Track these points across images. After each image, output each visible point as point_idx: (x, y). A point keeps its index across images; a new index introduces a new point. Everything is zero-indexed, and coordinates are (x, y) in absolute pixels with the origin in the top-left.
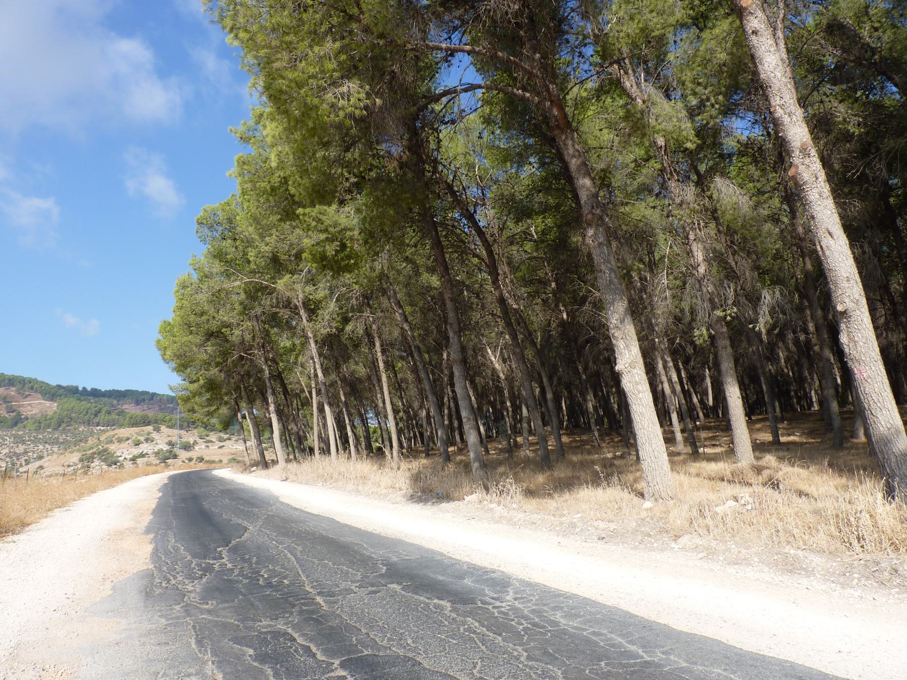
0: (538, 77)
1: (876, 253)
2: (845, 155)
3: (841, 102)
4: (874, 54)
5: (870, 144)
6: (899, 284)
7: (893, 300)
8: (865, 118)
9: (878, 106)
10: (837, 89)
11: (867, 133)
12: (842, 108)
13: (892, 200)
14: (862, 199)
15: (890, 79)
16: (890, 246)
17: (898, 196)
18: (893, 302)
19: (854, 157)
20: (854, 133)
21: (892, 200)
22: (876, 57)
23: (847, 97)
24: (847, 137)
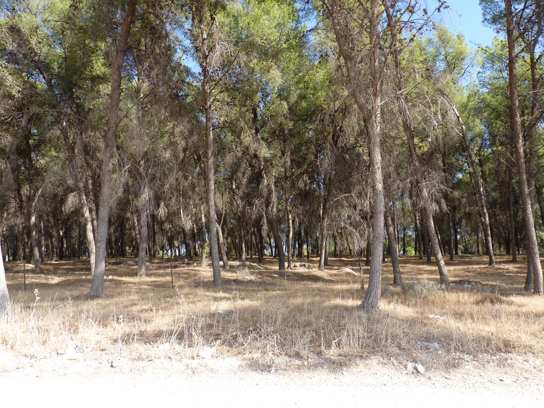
0: (171, 67)
1: (16, 170)
2: (7, 107)
3: (10, 74)
4: (35, 56)
5: (24, 105)
6: (27, 190)
7: (22, 199)
8: (24, 89)
9: (33, 86)
10: (10, 66)
11: (23, 99)
12: (10, 78)
13: (31, 141)
14: (14, 135)
15: (42, 73)
16: (25, 167)
17: (35, 140)
18: (21, 201)
19: (12, 109)
20: (14, 95)
21: (31, 141)
22: (36, 58)
23: (16, 73)
24: (11, 97)
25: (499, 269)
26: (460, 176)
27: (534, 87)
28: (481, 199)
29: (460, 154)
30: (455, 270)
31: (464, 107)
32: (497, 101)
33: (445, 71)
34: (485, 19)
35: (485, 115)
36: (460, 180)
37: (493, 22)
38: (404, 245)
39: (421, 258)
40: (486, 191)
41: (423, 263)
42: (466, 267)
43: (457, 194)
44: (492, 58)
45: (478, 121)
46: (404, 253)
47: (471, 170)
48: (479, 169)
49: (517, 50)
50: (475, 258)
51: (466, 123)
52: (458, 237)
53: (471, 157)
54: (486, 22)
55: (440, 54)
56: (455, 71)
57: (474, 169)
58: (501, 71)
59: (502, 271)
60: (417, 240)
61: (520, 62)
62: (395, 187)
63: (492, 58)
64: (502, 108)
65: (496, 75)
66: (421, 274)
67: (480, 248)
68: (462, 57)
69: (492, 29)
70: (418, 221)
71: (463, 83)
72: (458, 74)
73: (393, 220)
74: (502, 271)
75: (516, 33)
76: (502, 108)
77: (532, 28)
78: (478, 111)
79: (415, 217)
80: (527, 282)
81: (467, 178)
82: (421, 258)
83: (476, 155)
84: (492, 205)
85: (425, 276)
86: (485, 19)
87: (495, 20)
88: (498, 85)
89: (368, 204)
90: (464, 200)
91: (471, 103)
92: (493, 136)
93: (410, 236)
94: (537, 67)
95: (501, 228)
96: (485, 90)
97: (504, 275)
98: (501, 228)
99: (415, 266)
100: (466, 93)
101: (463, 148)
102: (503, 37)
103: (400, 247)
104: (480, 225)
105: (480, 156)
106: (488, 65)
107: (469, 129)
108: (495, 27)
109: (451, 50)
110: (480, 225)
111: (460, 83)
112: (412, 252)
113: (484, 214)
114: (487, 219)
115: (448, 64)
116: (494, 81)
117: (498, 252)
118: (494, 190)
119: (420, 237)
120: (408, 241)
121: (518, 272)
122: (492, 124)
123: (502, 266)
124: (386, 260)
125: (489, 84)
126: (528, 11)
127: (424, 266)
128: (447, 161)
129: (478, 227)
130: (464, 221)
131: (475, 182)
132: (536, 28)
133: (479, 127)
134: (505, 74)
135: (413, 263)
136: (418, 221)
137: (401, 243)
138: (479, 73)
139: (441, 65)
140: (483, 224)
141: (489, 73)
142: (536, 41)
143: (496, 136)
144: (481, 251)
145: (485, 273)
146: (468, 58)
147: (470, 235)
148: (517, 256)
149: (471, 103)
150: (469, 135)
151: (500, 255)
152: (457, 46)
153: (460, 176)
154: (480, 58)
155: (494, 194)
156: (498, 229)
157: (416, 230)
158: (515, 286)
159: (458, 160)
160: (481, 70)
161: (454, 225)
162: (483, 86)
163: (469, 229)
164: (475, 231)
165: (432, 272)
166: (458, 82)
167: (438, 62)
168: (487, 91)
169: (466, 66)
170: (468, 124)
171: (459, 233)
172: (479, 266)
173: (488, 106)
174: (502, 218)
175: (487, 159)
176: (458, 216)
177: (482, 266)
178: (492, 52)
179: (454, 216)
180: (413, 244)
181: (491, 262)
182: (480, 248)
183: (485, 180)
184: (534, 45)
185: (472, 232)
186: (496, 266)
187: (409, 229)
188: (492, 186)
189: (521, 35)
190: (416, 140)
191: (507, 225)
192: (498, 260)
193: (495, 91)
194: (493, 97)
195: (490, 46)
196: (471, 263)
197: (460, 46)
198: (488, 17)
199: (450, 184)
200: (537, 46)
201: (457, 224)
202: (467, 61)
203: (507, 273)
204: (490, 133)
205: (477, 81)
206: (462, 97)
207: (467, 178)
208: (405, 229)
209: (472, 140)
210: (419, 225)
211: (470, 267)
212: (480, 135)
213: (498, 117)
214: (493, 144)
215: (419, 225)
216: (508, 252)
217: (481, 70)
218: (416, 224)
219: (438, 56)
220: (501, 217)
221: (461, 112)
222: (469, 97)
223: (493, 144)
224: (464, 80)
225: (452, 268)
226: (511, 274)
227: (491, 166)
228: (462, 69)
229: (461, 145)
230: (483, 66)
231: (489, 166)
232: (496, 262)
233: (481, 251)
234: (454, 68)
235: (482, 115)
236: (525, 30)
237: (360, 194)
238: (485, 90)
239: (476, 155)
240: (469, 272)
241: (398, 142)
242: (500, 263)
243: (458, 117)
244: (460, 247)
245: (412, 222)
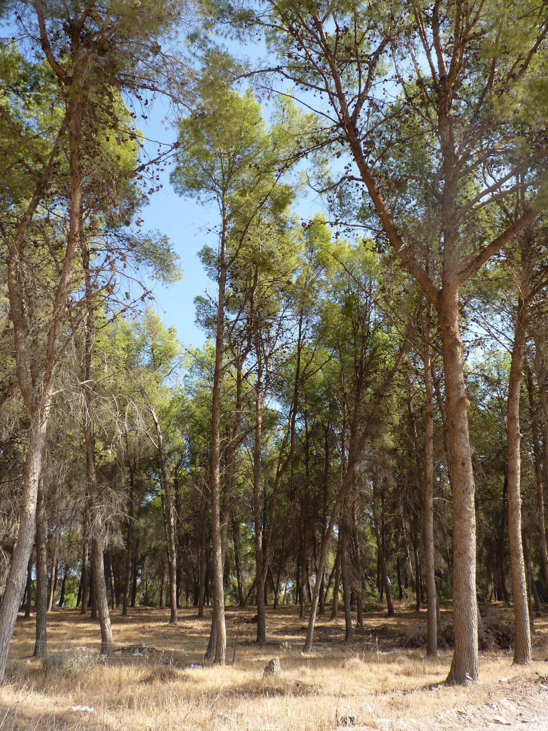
25: (182, 627)
26: (149, 498)
27: (238, 406)
28: (170, 533)
29: (154, 470)
30: (126, 630)
31: (164, 413)
32: (202, 413)
33: (148, 366)
34: (198, 320)
35: (188, 426)
36: (149, 504)
37: (206, 325)
38: (63, 592)
39: (83, 612)
40: (178, 522)
41: (85, 620)
42: (141, 625)
43: (142, 522)
44: (201, 363)
45: (178, 433)
46: (60, 605)
47: (163, 492)
48: (173, 491)
49: (225, 361)
50: (156, 613)
51: (165, 433)
52: (139, 581)
53: (165, 477)
54: (199, 323)
55: (146, 344)
56: (161, 368)
57: (166, 492)
58: (208, 379)
59: (184, 631)
60: (82, 584)
61: (227, 376)
62: (63, 505)
63: (201, 363)
64: (206, 423)
65: (204, 382)
66: (78, 638)
67: (164, 597)
68: (170, 354)
69: (204, 333)
70: (87, 557)
71: (168, 383)
72: (164, 372)
73: (50, 555)
74: (184, 631)
75: (225, 343)
76: (206, 423)
77: (242, 342)
78: (181, 420)
79: (84, 550)
80: (210, 647)
81: (158, 502)
82: (83, 612)
83: (172, 472)
84: (183, 540)
85: (84, 641)
86: (198, 320)
87: (208, 323)
88: (204, 395)
89: (18, 528)
90: (151, 531)
91: (174, 410)
92: (193, 454)
93: (74, 578)
94: (243, 384)
95: (191, 571)
96: (190, 397)
97: (186, 637)
98: (191, 571)
99: (73, 625)
100: (169, 397)
101: (158, 463)
102: (213, 343)
103: (56, 593)
104: (166, 565)
105: (176, 475)
106: (197, 370)
107: (167, 440)
108: (207, 330)
109: (159, 343)
110: (166, 565)
111: (164, 384)
112: (73, 600)
113: (172, 553)
114: (175, 561)
115: (154, 359)
116: (201, 389)
117: (183, 603)
118: (187, 520)
119: (87, 578)
120: (70, 585)
121: (202, 632)
122: (193, 438)
123: (184, 624)
124: (31, 615)
125: (195, 391)
126: (240, 323)
127: (85, 625)
128: (137, 477)
129: (164, 568)
130: (147, 559)
131: (166, 508)
132: (245, 343)
133: (180, 440)
134: (212, 384)
135: (70, 620)
136: (87, 557)
137: (59, 588)
138: (186, 376)
139: (145, 358)
140: (170, 564)
141: (196, 379)
142: (244, 357)
143: (196, 453)
144: (164, 600)
145: (164, 633)
146: (177, 357)
147: (153, 578)
148: (204, 610)
149: (174, 410)
150: (167, 448)
151: (186, 607)
152: (166, 339)
153: (149, 498)
154: (190, 360)
155: (186, 526)
156: (187, 571)
157: (83, 570)
158: (196, 652)
159: (149, 476)
160: (188, 374)
161: (135, 564)
162: (189, 393)
163: (153, 571)
164: (160, 573)
165: (94, 634)
166: (162, 381)
167: (142, 353)
168: (193, 398)
169: (173, 366)
170: (167, 434)
171: (139, 575)
172: (158, 624)
173: (191, 416)
174: (193, 558)
175: (185, 480)
176: (141, 552)
177: (162, 624)
178: (202, 355)
179: (136, 552)
180: (76, 590)
181: (172, 619)
182: (164, 597)
183: (178, 507)
184: (242, 361)
185: (157, 574)
186: (179, 623)
187: (74, 566)
188: (186, 516)
189: (231, 347)
190: (99, 445)
191: (197, 567)
192: (183, 615)
193: (200, 400)
194: (197, 407)
195: (201, 349)
196: (149, 619)
197: (170, 341)
198: (202, 318)
199: (136, 508)
200: (245, 362)
201: (138, 562)
202: (175, 360)
203: (190, 633)
204: (191, 450)
205: (183, 386)
206: (164, 401)
207: (158, 502)
208: (67, 568)
209: (169, 454)
210: (87, 562)
211: (147, 624)
212: (178, 450)
213: (201, 431)
214: (193, 463)
215: (87, 562)
216: (195, 604)
217: (188, 374)
218: (84, 560)
219: (144, 345)
220: (193, 556)
221: (161, 418)
222: (171, 403)
223: (193, 463)
224: (169, 381)
225: (123, 627)
226: (195, 635)
227: (187, 490)
228: (168, 367)
229: (156, 459)
230: (191, 370)
231: (184, 489)
232: (179, 619)
233: (164, 600)
234: (160, 364)
235: (184, 426)
236: (235, 342)
237: (9, 511)
238: (190, 397)
239: (172, 472)
240: (144, 633)
241: (76, 444)
242: (184, 619)
243: (156, 424)
244: (140, 595)
245: (78, 557)
